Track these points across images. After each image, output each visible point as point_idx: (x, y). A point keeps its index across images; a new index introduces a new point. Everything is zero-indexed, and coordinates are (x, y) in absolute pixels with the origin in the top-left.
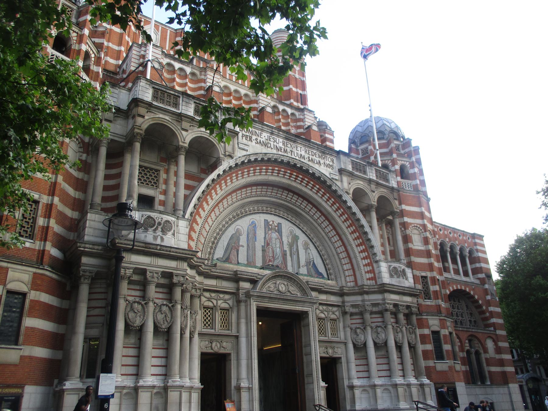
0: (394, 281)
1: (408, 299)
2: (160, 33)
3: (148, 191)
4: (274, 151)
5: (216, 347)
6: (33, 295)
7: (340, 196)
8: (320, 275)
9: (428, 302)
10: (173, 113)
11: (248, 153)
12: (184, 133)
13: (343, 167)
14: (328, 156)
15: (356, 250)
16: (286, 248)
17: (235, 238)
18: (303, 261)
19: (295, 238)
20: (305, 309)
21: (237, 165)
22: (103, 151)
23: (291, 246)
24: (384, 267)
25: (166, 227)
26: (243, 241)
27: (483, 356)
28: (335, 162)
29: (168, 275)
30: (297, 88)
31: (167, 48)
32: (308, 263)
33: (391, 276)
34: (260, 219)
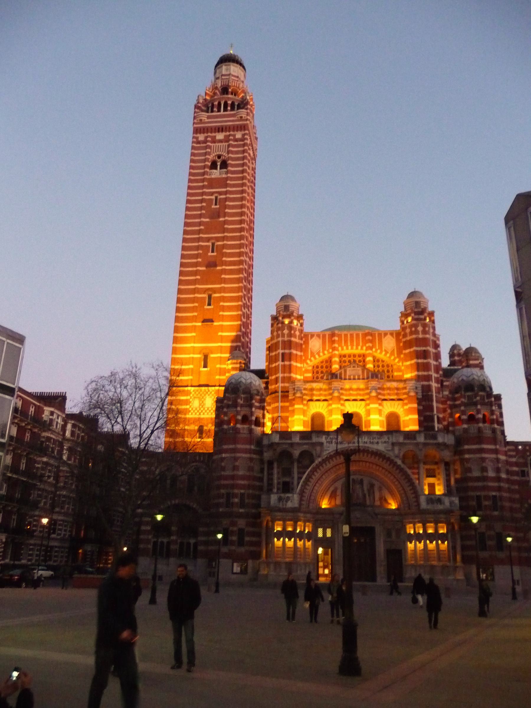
0: (430, 507)
2: (321, 340)
3: (287, 479)
4: (346, 445)
6: (247, 529)
7: (393, 460)
10: (289, 444)
11: (330, 451)
12: (295, 452)
13: (394, 441)
14: (385, 436)
15: (408, 489)
16: (366, 492)
19: (372, 486)
20: (373, 525)
21: (323, 460)
23: (369, 491)
25: (288, 499)
28: (390, 438)
30: (420, 347)
31: (327, 349)
33: (428, 503)
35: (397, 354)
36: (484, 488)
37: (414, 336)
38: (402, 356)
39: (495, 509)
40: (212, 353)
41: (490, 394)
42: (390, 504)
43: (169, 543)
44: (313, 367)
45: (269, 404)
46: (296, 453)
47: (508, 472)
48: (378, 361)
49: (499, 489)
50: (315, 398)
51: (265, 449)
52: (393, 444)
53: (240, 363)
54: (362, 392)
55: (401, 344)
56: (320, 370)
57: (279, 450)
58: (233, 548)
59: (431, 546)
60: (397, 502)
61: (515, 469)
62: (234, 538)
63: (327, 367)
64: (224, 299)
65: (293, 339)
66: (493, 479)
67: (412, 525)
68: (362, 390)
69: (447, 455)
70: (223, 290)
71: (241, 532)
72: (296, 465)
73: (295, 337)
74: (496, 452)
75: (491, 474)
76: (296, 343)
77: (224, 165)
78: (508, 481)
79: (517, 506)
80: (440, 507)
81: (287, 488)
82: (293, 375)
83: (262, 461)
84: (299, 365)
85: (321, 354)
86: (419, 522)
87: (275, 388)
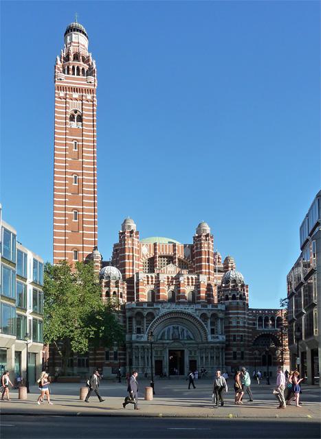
0: (212, 340)
1: (218, 345)
3: (138, 327)
5: (159, 359)
8: (191, 339)
9: (235, 343)
15: (202, 331)
17: (164, 333)
18: (185, 335)
22: (127, 320)
24: (209, 337)
25: (142, 337)
26: (166, 333)
27: (272, 357)
29: (143, 347)
32: (187, 336)
34: (171, 327)
36: (237, 331)
39: (242, 341)
41: (243, 286)
43: (72, 360)
46: (145, 313)
47: (248, 324)
49: (244, 332)
51: (127, 311)
52: (196, 310)
57: (136, 311)
58: (112, 361)
61: (251, 322)
62: (112, 356)
66: (241, 327)
69: (221, 315)
71: (116, 354)
72: (145, 319)
74: (244, 314)
75: (241, 324)
77: (80, 119)
78: (248, 328)
79: (250, 339)
80: (218, 340)
81: (139, 331)
83: (125, 317)
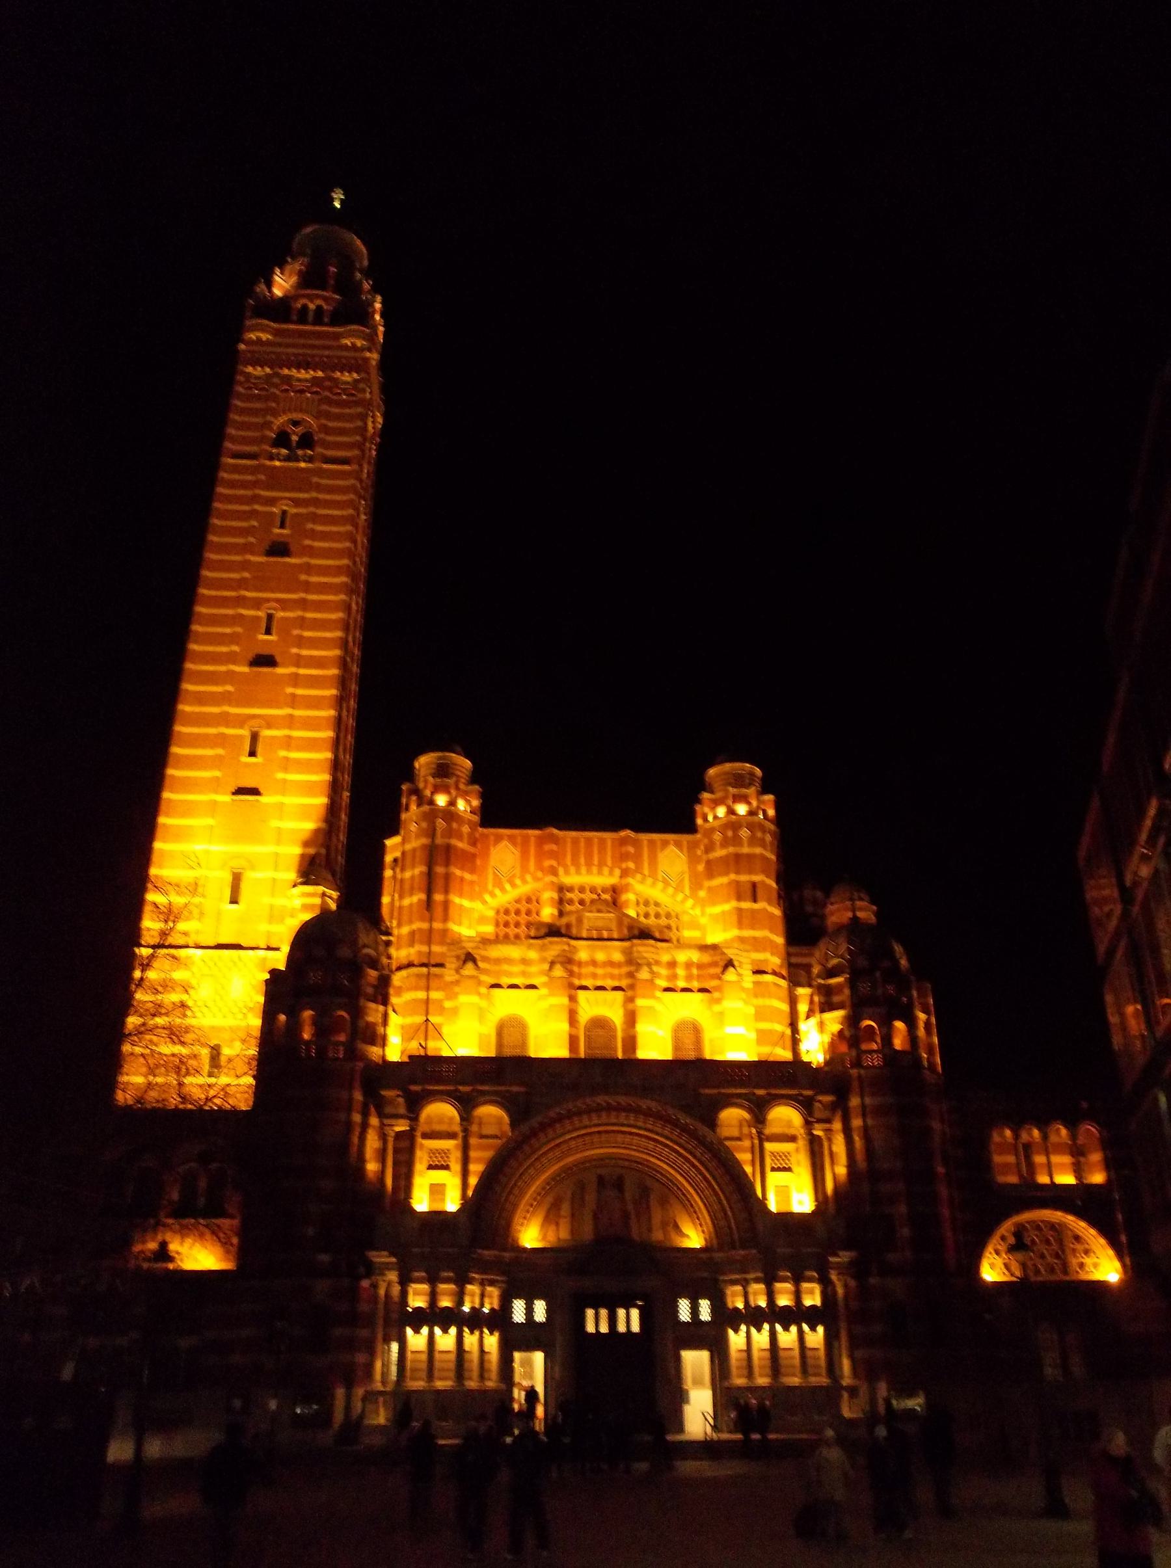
35: (691, 888)
37: (731, 849)
38: (702, 894)
40: (253, 867)
42: (687, 1236)
44: (498, 912)
45: (399, 991)
48: (646, 903)
50: (506, 981)
53: (324, 895)
54: (616, 971)
55: (701, 868)
56: (512, 918)
59: (788, 1338)
60: (703, 1232)
63: (528, 913)
64: (288, 743)
65: (455, 842)
67: (739, 1288)
68: (618, 965)
70: (290, 722)
73: (460, 837)
76: (463, 850)
82: (455, 928)
84: (466, 903)
85: (518, 882)
86: (757, 1281)
87: (409, 955)
